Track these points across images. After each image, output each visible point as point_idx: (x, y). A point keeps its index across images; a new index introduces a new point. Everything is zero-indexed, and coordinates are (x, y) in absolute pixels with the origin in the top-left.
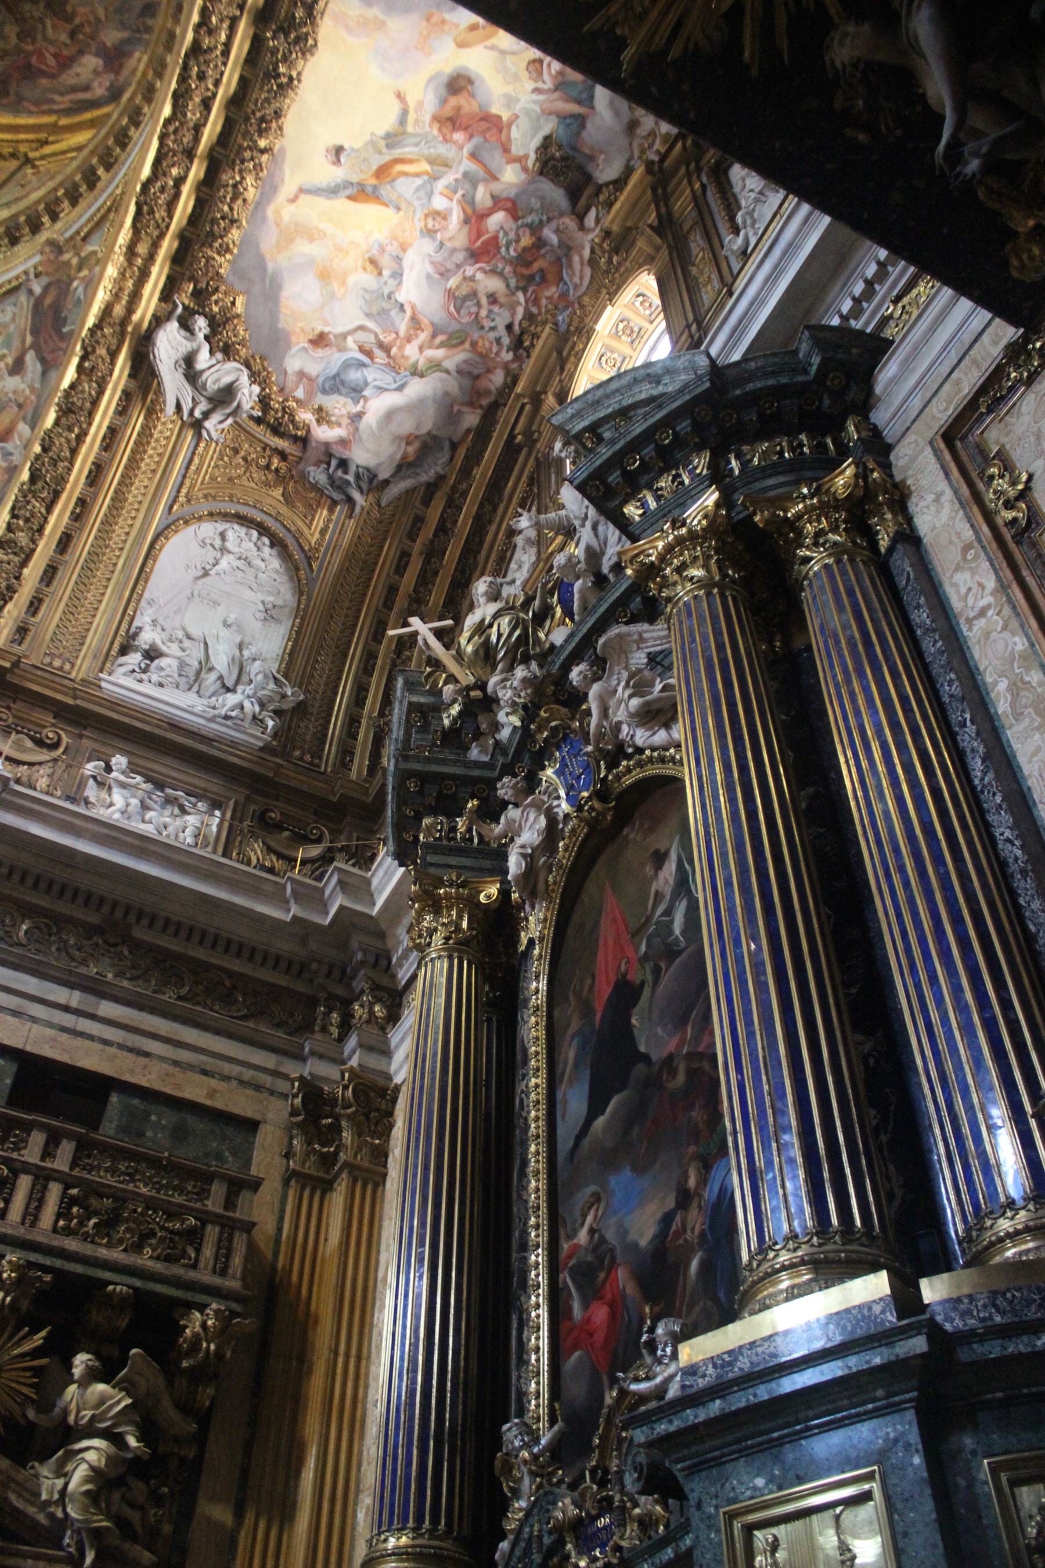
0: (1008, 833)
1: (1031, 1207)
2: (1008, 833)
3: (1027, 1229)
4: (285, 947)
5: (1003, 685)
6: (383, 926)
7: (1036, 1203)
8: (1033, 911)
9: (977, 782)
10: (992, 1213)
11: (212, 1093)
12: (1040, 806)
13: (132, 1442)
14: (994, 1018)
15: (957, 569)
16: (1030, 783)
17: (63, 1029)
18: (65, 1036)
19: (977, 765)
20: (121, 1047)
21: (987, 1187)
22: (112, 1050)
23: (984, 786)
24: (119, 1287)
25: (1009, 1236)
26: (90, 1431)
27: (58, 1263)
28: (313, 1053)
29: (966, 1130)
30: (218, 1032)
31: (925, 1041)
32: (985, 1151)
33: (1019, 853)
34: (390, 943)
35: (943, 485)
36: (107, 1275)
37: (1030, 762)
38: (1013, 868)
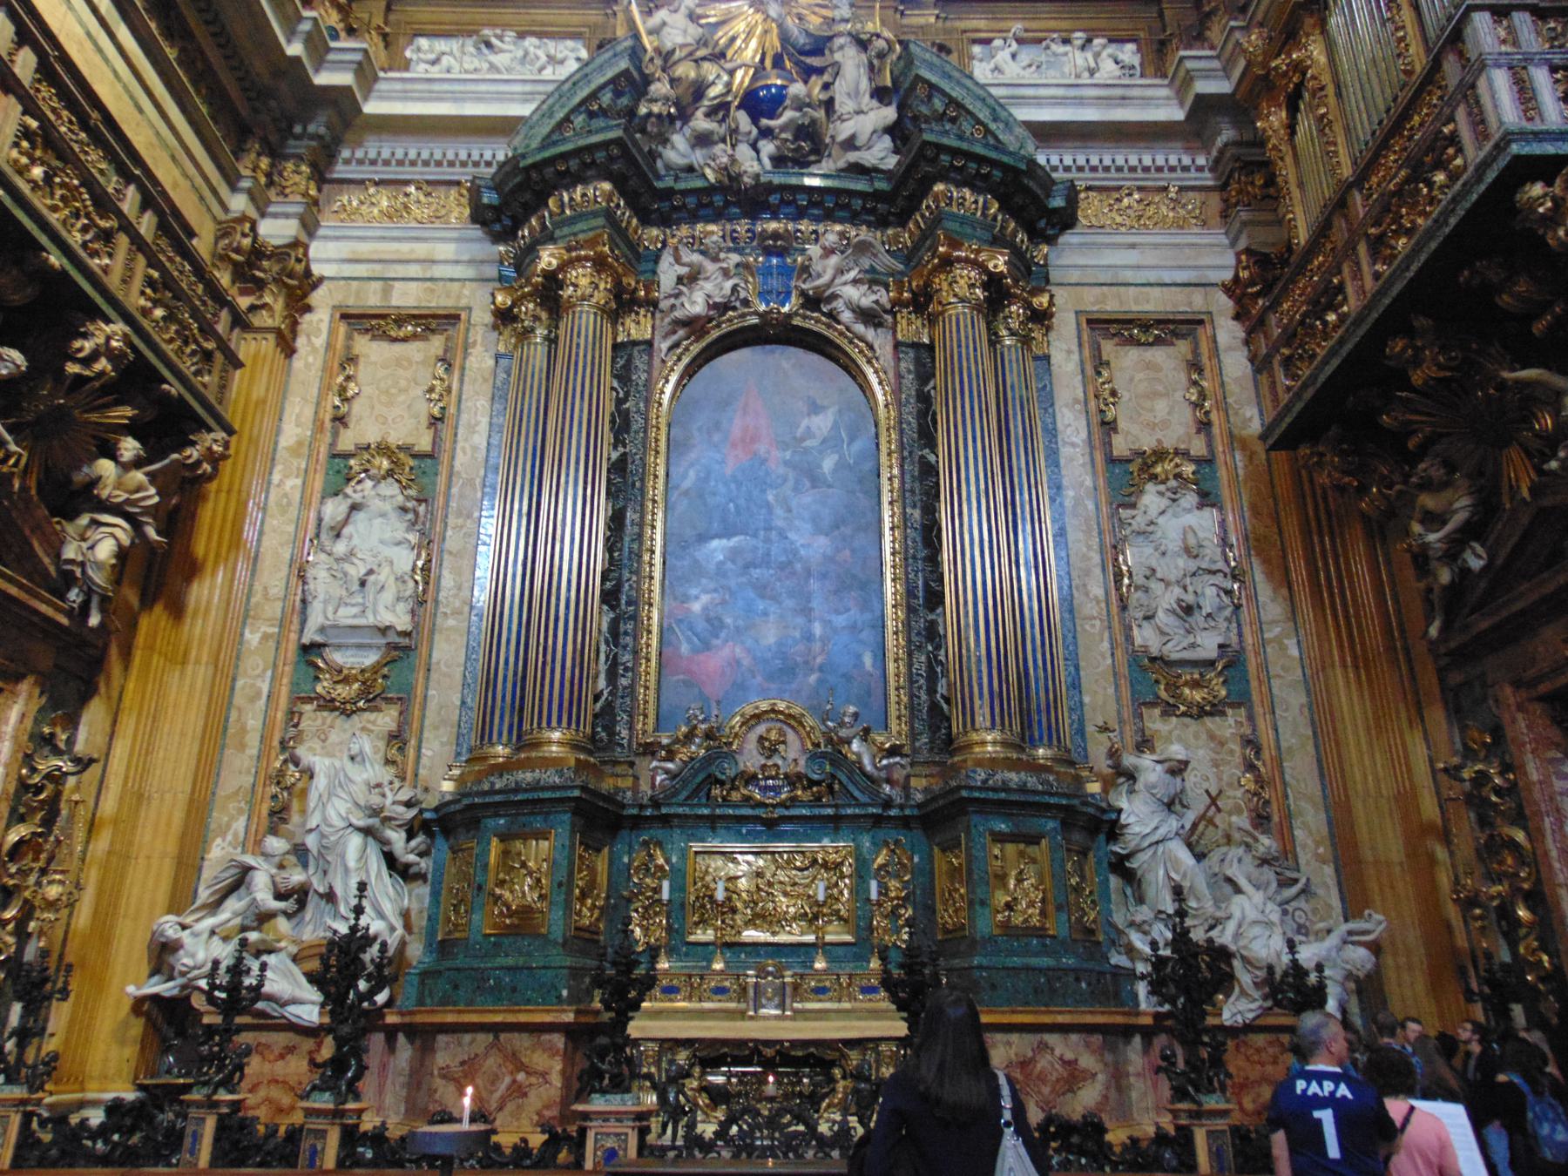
4: (259, 66)
5: (1071, 493)
6: (358, 121)
11: (175, 185)
13: (151, 532)
15: (1066, 406)
17: (89, 34)
18: (89, 45)
20: (125, 87)
22: (119, 87)
24: (173, 388)
26: (117, 510)
27: (141, 346)
28: (249, 192)
30: (192, 122)
34: (349, 136)
35: (1075, 348)
36: (166, 373)
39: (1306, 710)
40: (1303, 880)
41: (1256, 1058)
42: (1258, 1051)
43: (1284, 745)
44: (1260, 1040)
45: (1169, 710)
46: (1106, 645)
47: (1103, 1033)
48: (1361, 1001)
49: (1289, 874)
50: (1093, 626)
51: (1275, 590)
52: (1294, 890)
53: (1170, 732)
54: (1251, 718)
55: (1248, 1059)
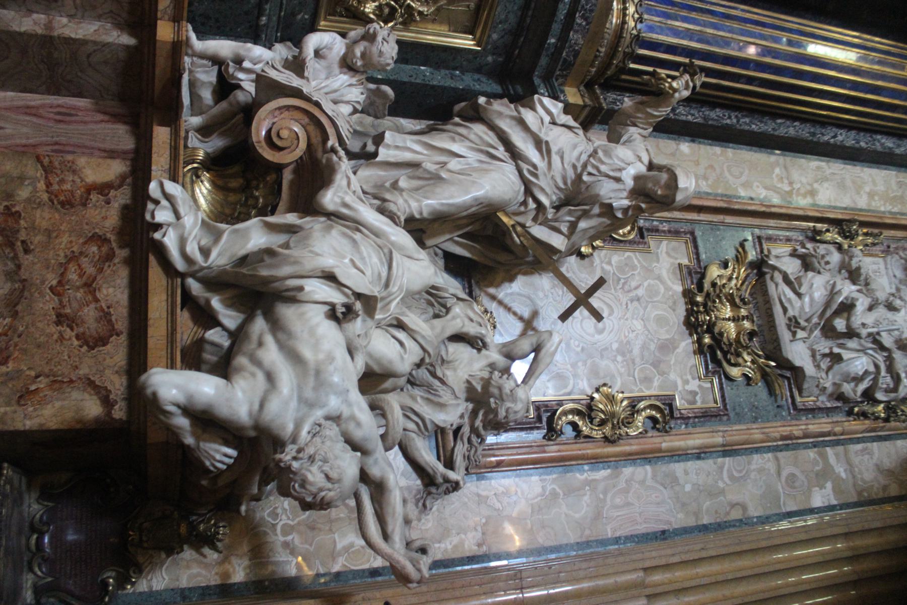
0: (840, 138)
1: (634, 32)
2: (840, 138)
3: (624, 22)
7: (635, 36)
8: (788, 127)
9: (879, 137)
10: (641, 5)
12: (842, 166)
14: (747, 68)
16: (858, 168)
19: (889, 143)
21: (656, 10)
23: (874, 140)
25: (625, 9)
29: (693, 15)
31: (756, 17)
32: (677, 20)
33: (826, 138)
37: (870, 175)
38: (818, 130)
39: (736, 515)
40: (452, 475)
41: (73, 276)
42: (90, 286)
43: (678, 468)
44: (115, 291)
45: (695, 277)
46: (762, 193)
47: (137, 151)
48: (205, 591)
49: (460, 450)
50: (781, 179)
51: (890, 473)
52: (427, 455)
53: (659, 278)
54: (706, 416)
55: (73, 258)
